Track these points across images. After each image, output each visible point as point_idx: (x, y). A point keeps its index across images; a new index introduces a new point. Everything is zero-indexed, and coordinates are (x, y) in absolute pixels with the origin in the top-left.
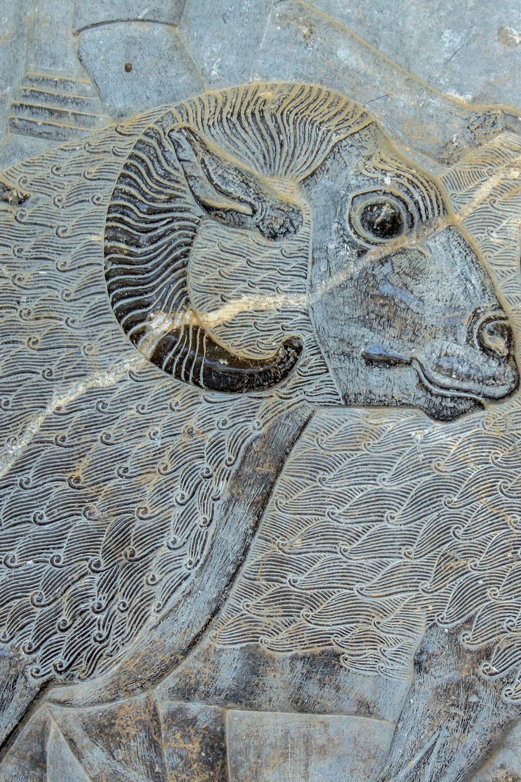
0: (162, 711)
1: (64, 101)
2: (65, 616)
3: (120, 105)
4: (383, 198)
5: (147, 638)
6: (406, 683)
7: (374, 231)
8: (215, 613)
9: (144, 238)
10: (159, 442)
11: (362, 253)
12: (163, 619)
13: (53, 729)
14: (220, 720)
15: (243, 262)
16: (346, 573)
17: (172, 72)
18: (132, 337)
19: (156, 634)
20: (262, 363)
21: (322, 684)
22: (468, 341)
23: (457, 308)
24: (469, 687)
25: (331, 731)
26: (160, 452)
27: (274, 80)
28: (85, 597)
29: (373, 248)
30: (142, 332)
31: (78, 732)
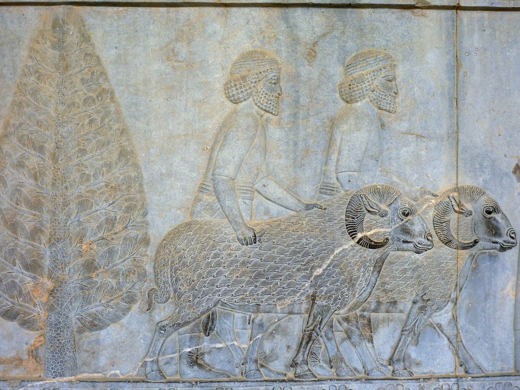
0: (358, 315)
1: (334, 188)
3: (347, 189)
4: (407, 209)
5: (356, 300)
7: (405, 216)
8: (370, 294)
9: (355, 217)
10: (358, 260)
11: (402, 220)
12: (359, 296)
14: (370, 316)
15: (375, 222)
16: (398, 285)
17: (358, 182)
18: (352, 238)
19: (358, 299)
20: (381, 243)
21: (393, 307)
22: (425, 237)
23: (422, 231)
24: (426, 307)
25: (393, 316)
26: (358, 261)
27: (379, 184)
29: (405, 219)
30: (355, 237)
31: (341, 320)
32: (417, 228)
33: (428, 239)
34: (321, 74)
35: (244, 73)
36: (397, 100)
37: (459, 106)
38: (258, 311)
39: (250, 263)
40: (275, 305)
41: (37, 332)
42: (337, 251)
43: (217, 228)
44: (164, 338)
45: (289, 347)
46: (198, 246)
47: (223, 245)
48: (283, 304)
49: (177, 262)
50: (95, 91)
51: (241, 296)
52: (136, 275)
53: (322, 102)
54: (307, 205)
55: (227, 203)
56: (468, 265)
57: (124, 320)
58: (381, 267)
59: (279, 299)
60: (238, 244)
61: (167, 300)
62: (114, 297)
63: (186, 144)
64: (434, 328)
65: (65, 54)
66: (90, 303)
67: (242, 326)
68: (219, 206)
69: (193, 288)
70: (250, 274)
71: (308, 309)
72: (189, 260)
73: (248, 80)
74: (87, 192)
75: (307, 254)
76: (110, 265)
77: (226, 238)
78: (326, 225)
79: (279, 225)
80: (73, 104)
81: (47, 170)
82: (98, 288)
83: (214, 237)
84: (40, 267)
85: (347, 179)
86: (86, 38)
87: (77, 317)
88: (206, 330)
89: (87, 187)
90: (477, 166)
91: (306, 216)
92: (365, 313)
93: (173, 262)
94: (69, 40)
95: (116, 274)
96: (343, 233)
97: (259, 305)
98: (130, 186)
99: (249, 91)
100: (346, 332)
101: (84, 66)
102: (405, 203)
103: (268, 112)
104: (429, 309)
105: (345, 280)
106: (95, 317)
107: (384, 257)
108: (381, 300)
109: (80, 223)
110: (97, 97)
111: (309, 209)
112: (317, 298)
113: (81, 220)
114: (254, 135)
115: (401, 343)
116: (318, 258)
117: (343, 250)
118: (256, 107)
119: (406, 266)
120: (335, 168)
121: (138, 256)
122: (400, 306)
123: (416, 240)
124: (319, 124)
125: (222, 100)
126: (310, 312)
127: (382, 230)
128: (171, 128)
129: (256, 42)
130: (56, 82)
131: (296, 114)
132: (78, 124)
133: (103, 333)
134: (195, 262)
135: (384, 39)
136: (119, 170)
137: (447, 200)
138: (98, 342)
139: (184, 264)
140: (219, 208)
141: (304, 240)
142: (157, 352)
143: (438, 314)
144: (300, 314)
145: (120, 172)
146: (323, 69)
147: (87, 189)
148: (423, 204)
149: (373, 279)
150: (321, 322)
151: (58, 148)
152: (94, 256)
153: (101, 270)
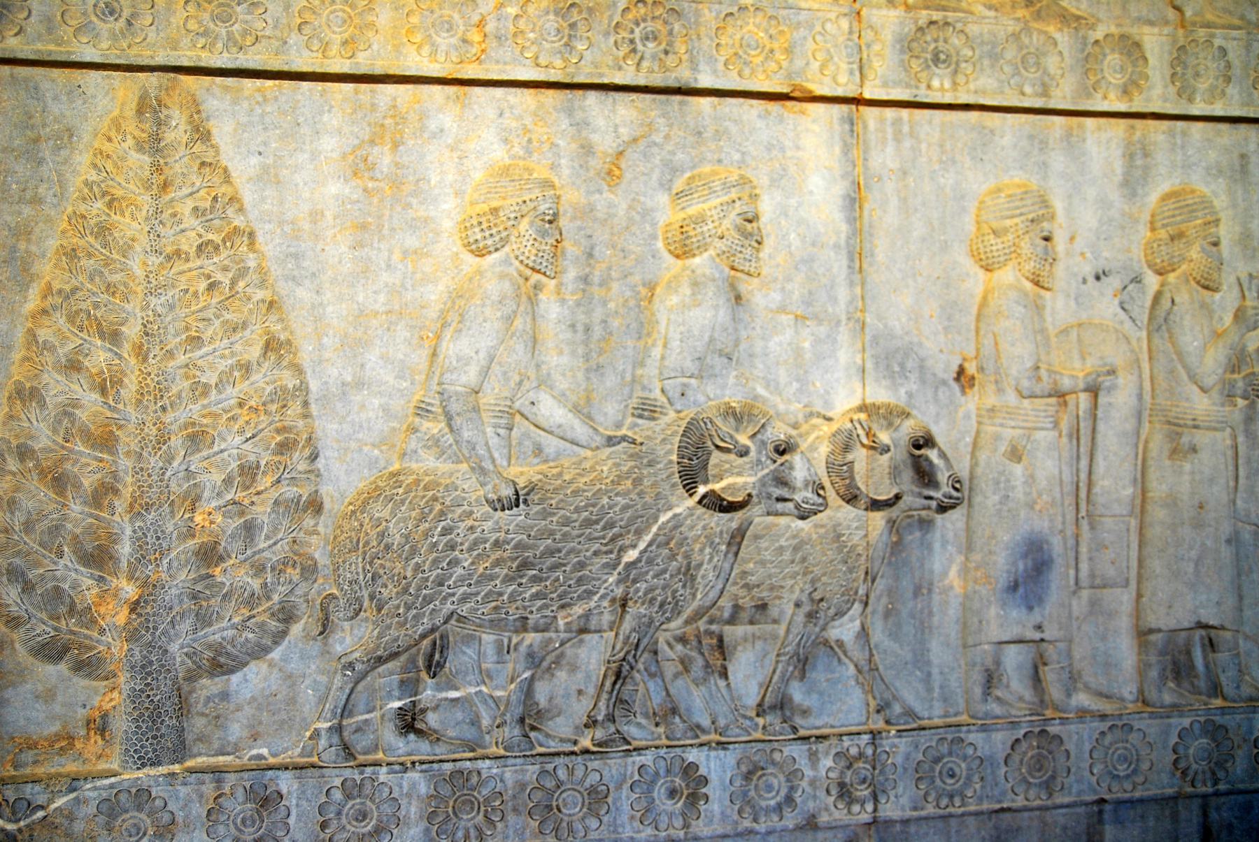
0: (702, 629)
2: (670, 599)
3: (679, 408)
6: (790, 612)
11: (775, 462)
13: (661, 640)
15: (727, 466)
28: (676, 591)
31: (671, 640)
32: (799, 473)
33: (819, 495)
34: (630, 207)
35: (495, 204)
36: (761, 255)
37: (865, 266)
38: (525, 629)
39: (508, 543)
40: (555, 617)
41: (105, 683)
42: (663, 518)
43: (448, 481)
44: (350, 685)
45: (580, 692)
46: (414, 514)
47: (459, 511)
48: (570, 615)
49: (375, 543)
50: (219, 231)
51: (493, 604)
52: (298, 570)
53: (633, 256)
54: (610, 438)
55: (466, 434)
56: (884, 538)
57: (276, 655)
58: (740, 544)
59: (563, 607)
60: (487, 508)
61: (357, 615)
62: (255, 612)
63: (389, 329)
64: (831, 648)
65: (162, 161)
66: (210, 625)
67: (495, 658)
68: (451, 441)
69: (405, 591)
70: (509, 564)
71: (614, 622)
72: (397, 539)
73: (501, 214)
74: (203, 416)
75: (611, 525)
76: (249, 552)
77: (464, 499)
78: (645, 472)
79: (560, 474)
80: (178, 253)
81: (126, 375)
82: (225, 596)
83: (443, 497)
84: (111, 558)
85: (679, 390)
86: (201, 134)
87: (185, 650)
88: (429, 667)
89: (204, 407)
90: (897, 369)
91: (608, 458)
92: (714, 627)
93: (367, 543)
94: (169, 136)
95: (259, 569)
96: (674, 485)
97: (527, 618)
98: (285, 406)
99: (504, 234)
100: (682, 662)
101: (198, 184)
102: (778, 432)
103: (538, 271)
104: (821, 614)
105: (679, 569)
106: (218, 649)
107: (744, 527)
108: (741, 602)
109: (189, 474)
110: (224, 241)
111: (614, 445)
112: (630, 603)
113: (192, 468)
114: (515, 312)
115: (776, 678)
116: (629, 532)
117: (675, 516)
118: (517, 263)
119: (783, 542)
120: (657, 371)
121: (302, 534)
122: (774, 612)
123: (798, 497)
124: (628, 293)
125: (455, 249)
126: (618, 628)
127: (740, 480)
128: (361, 298)
129: (516, 149)
130: (144, 212)
131: (587, 276)
132: (187, 291)
133: (235, 678)
134: (407, 542)
135: (738, 151)
136: (265, 376)
137: (849, 425)
138: (225, 696)
139: (388, 547)
140: (451, 445)
141: (605, 500)
142: (339, 710)
143: (837, 623)
144: (599, 631)
145: (267, 379)
146: (634, 200)
147: (204, 412)
148: (808, 433)
149: (727, 566)
150: (637, 645)
151: (147, 335)
152: (217, 536)
153: (232, 562)
